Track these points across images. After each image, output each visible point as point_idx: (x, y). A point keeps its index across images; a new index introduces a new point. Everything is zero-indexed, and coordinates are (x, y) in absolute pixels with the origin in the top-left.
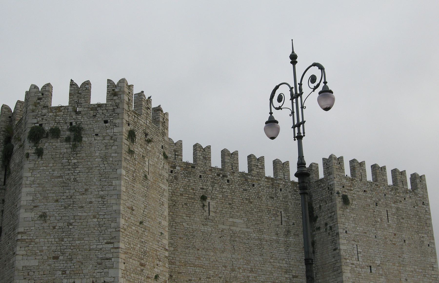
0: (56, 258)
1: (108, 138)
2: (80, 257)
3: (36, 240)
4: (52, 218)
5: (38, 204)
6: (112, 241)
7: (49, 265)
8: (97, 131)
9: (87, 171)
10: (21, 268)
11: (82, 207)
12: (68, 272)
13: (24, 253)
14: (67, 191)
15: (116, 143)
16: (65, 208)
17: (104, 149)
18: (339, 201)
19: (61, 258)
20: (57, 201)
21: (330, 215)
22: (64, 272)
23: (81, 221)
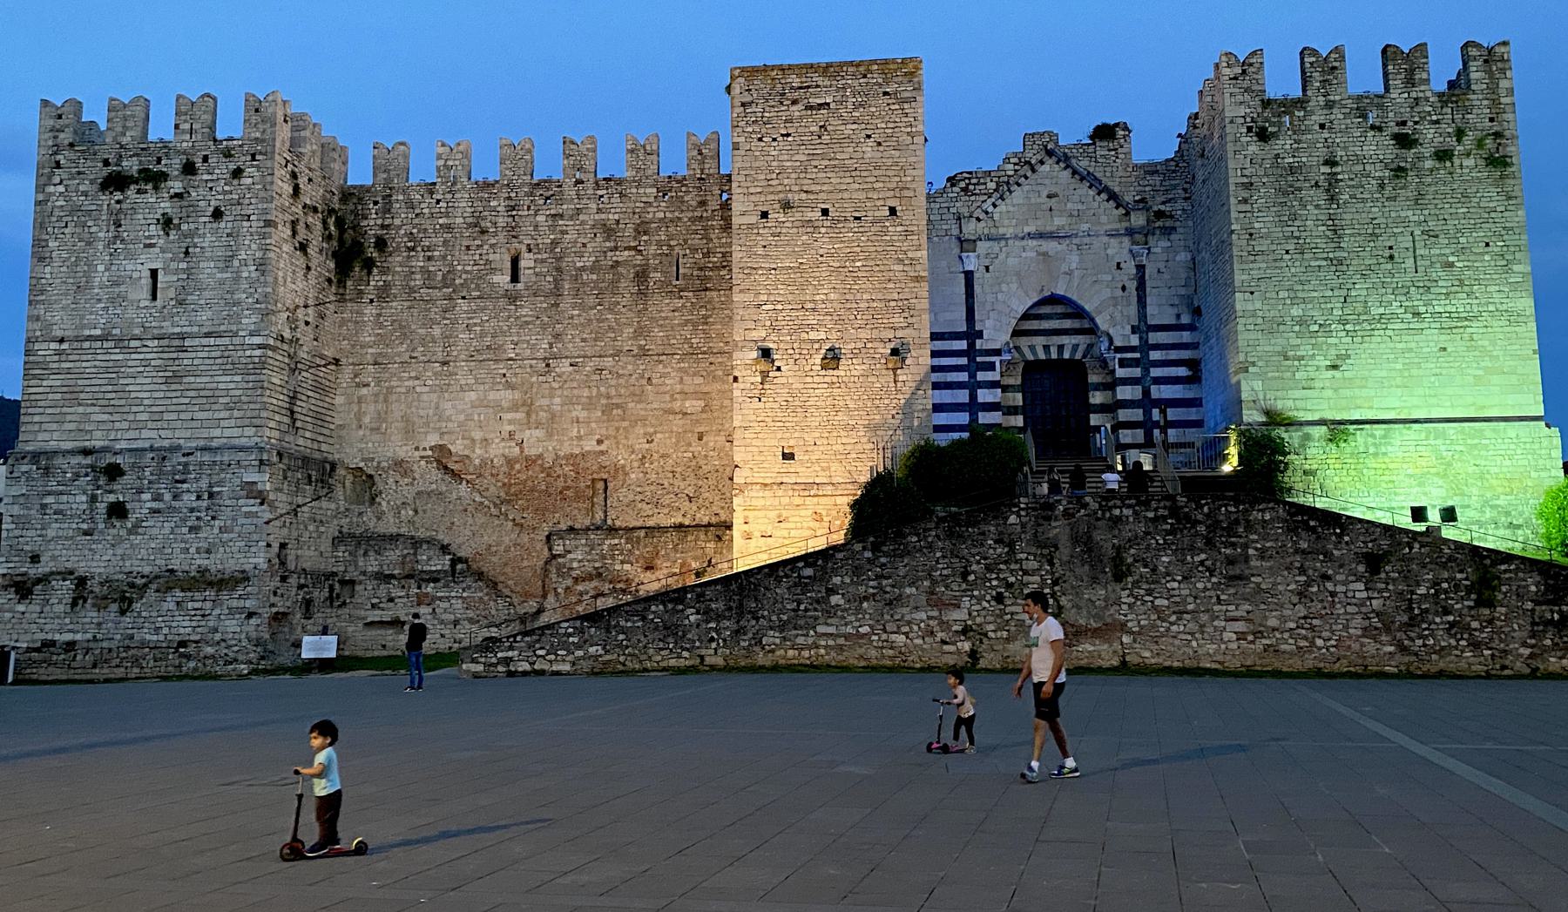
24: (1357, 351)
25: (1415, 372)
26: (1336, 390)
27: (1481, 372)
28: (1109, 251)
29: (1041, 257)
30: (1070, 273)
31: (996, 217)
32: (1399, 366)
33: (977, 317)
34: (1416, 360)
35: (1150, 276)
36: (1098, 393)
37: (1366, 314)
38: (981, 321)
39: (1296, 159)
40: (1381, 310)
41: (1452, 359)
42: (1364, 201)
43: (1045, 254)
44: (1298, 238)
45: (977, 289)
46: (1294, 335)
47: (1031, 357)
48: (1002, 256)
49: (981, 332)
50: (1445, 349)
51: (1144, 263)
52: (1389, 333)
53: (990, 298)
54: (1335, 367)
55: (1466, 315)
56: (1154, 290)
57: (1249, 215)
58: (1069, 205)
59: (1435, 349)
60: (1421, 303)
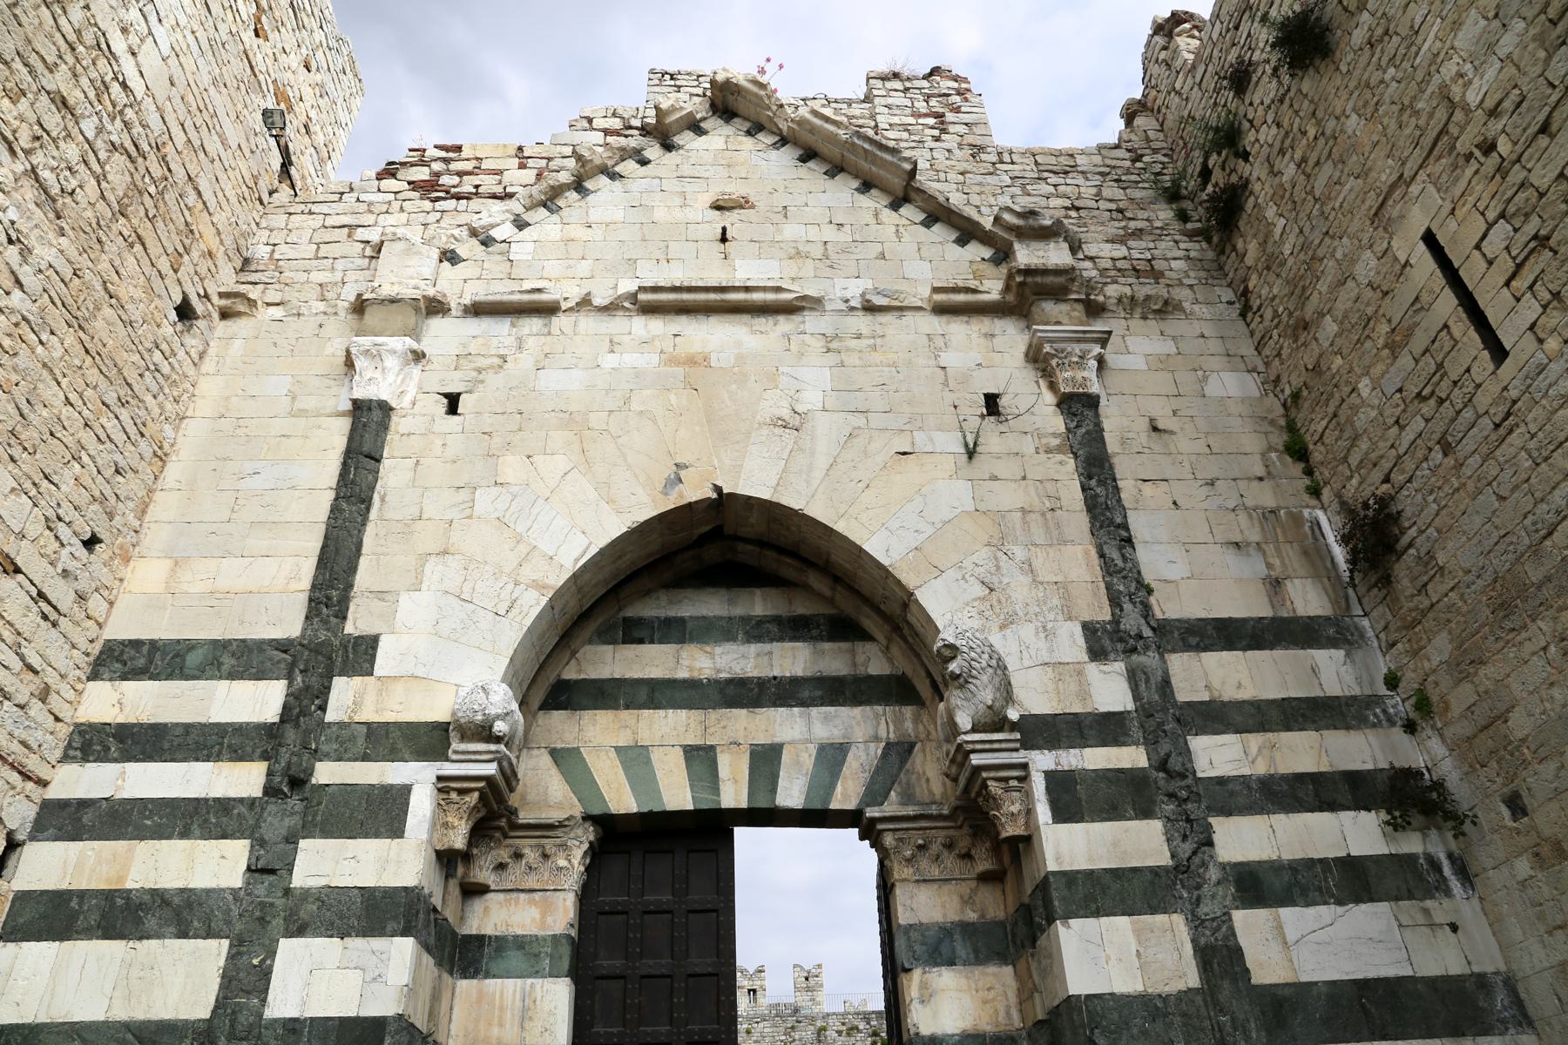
28: (947, 359)
29: (680, 371)
30: (792, 424)
31: (520, 251)
33: (364, 577)
35: (1123, 441)
36: (946, 980)
38: (381, 594)
43: (698, 363)
45: (393, 474)
47: (622, 800)
48: (522, 363)
49: (368, 646)
51: (1095, 388)
53: (438, 505)
56: (1148, 489)
58: (791, 231)
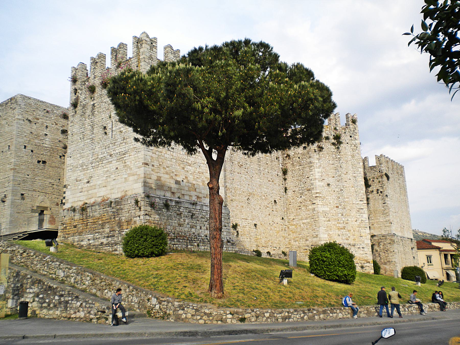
0: (337, 207)
1: (353, 145)
2: (349, 207)
3: (327, 197)
4: (332, 186)
5: (324, 178)
6: (362, 200)
7: (335, 211)
8: (347, 141)
9: (346, 162)
10: (321, 212)
11: (346, 181)
12: (344, 215)
13: (322, 204)
14: (338, 172)
15: (357, 149)
16: (338, 181)
17: (352, 151)
18: (385, 178)
19: (340, 207)
20: (333, 177)
21: (380, 185)
22: (342, 215)
23: (347, 189)
24: (94, 174)
25: (109, 180)
26: (88, 191)
27: (126, 176)
32: (105, 178)
34: (109, 175)
37: (98, 158)
39: (85, 101)
40: (102, 156)
41: (119, 172)
42: (101, 112)
44: (83, 132)
46: (79, 171)
50: (117, 168)
52: (103, 165)
54: (88, 182)
55: (124, 152)
57: (72, 127)
59: (115, 169)
60: (112, 150)
